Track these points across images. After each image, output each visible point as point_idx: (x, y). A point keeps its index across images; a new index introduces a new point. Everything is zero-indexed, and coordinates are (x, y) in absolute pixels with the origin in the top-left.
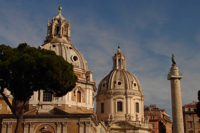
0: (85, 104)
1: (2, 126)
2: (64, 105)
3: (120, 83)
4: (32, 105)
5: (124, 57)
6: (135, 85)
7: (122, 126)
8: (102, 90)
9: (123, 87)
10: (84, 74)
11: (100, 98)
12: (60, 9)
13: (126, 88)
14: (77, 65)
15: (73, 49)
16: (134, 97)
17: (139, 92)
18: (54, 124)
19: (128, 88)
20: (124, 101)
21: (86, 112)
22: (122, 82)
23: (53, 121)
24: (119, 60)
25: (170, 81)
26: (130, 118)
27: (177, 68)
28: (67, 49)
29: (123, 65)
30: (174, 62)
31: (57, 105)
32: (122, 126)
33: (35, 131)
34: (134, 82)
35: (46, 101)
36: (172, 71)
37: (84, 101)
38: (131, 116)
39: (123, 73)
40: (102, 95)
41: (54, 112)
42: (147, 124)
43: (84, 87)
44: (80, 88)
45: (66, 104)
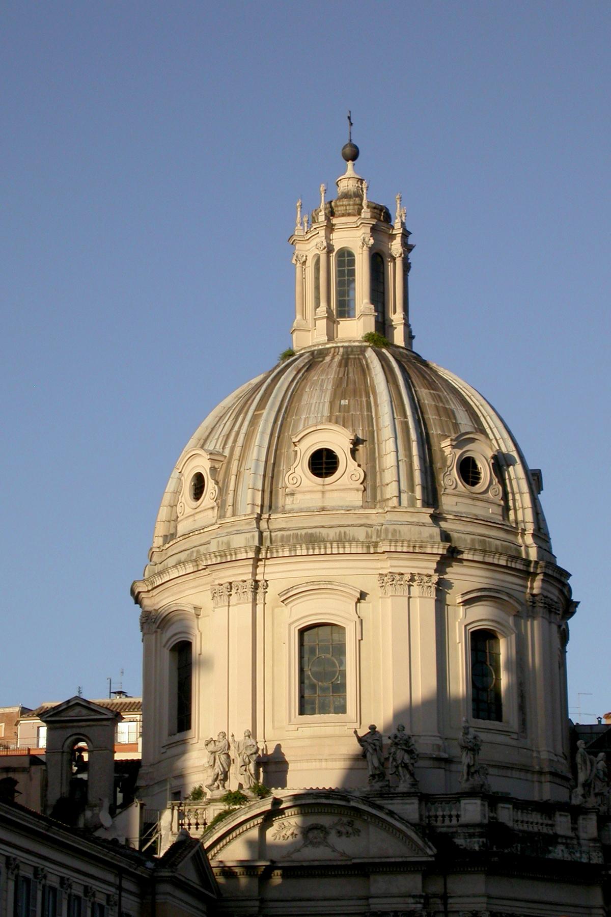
3: (323, 463)
7: (333, 838)
8: (182, 528)
26: (406, 766)
38: (410, 752)
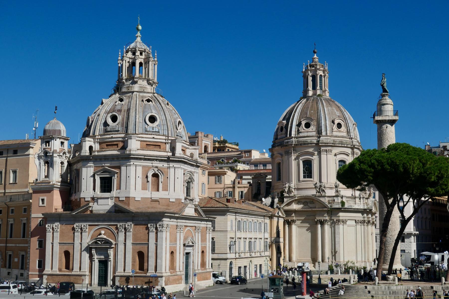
1: (46, 230)
2: (128, 198)
3: (308, 125)
4: (85, 198)
5: (324, 71)
6: (339, 126)
7: (309, 204)
8: (279, 137)
9: (315, 133)
10: (168, 144)
11: (275, 153)
13: (319, 132)
14: (154, 129)
15: (153, 101)
16: (336, 150)
17: (348, 139)
18: (113, 228)
19: (324, 133)
20: (315, 159)
21: (168, 205)
22: (312, 123)
24: (314, 78)
25: (376, 126)
26: (324, 191)
27: (388, 100)
28: (141, 102)
29: (321, 87)
31: (119, 198)
32: (309, 204)
33: (90, 237)
36: (380, 105)
37: (166, 189)
38: (325, 187)
39: (317, 103)
40: (277, 148)
41: (115, 210)
42: (360, 199)
44: (156, 170)
45: (131, 195)
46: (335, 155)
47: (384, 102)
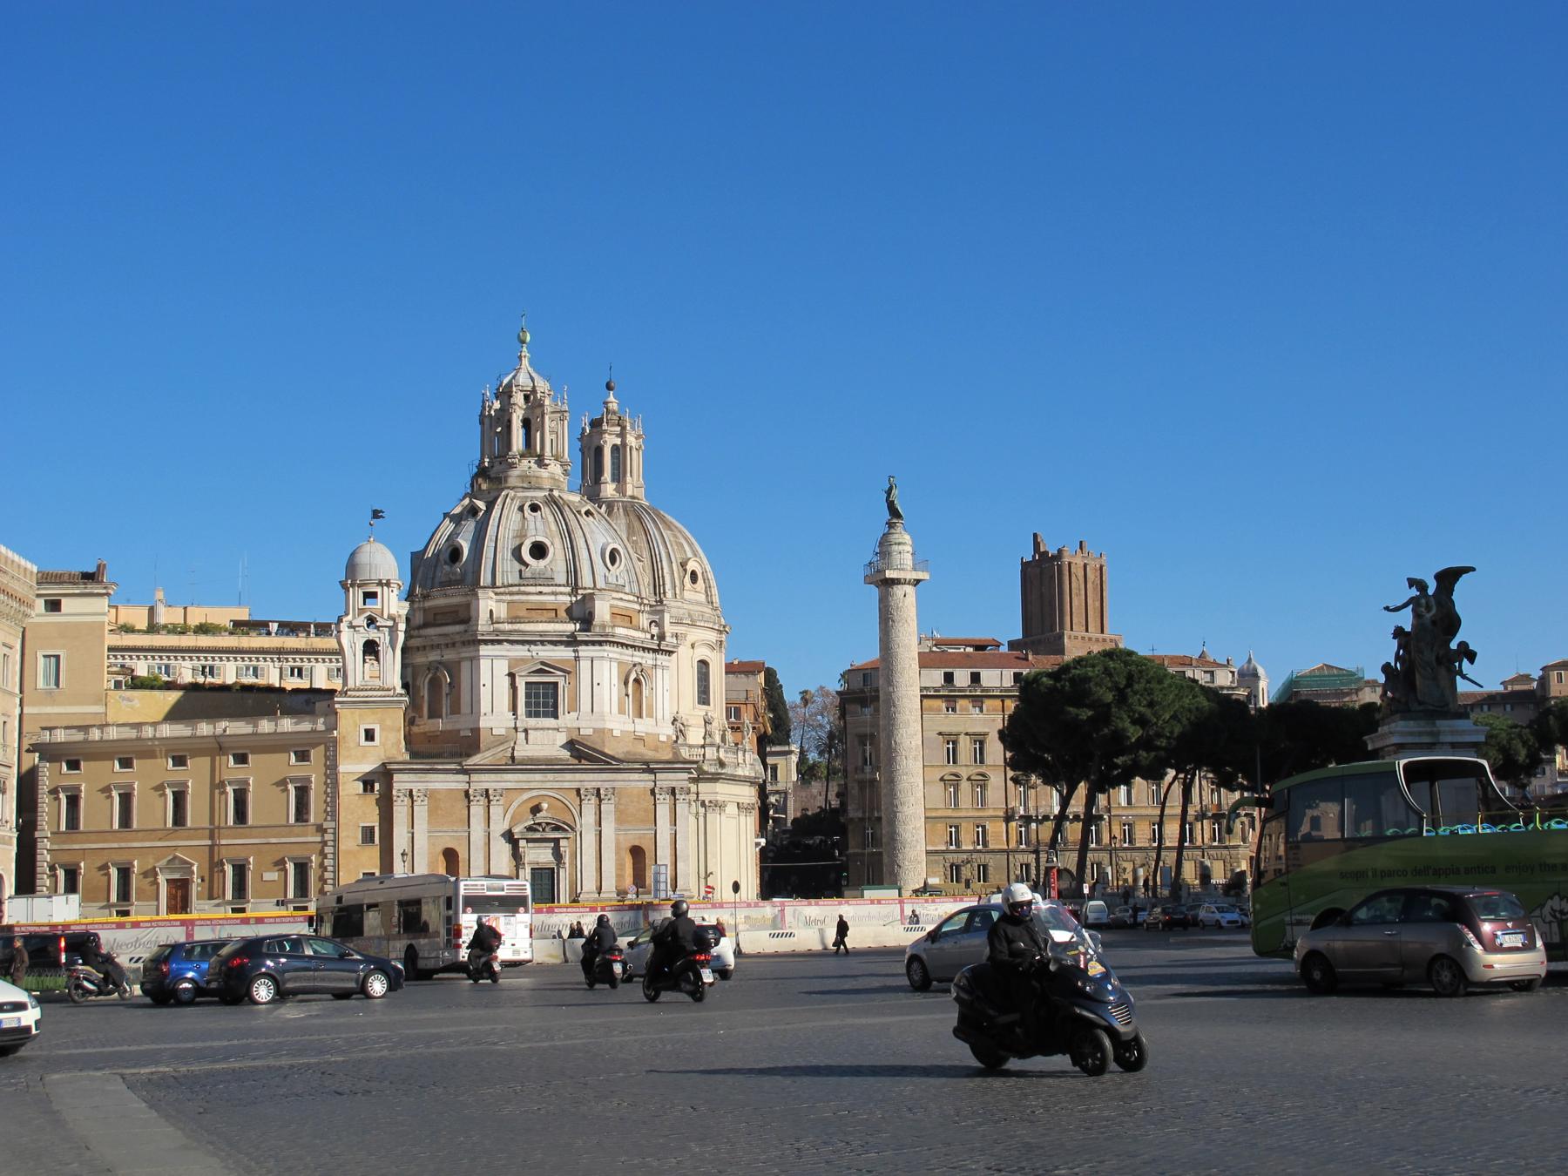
0: (651, 721)
12: (523, 342)
23: (566, 785)
25: (874, 591)
27: (907, 538)
30: (894, 513)
33: (508, 816)
34: (691, 566)
35: (537, 715)
39: (640, 518)
43: (650, 662)
46: (693, 646)
47: (895, 538)
